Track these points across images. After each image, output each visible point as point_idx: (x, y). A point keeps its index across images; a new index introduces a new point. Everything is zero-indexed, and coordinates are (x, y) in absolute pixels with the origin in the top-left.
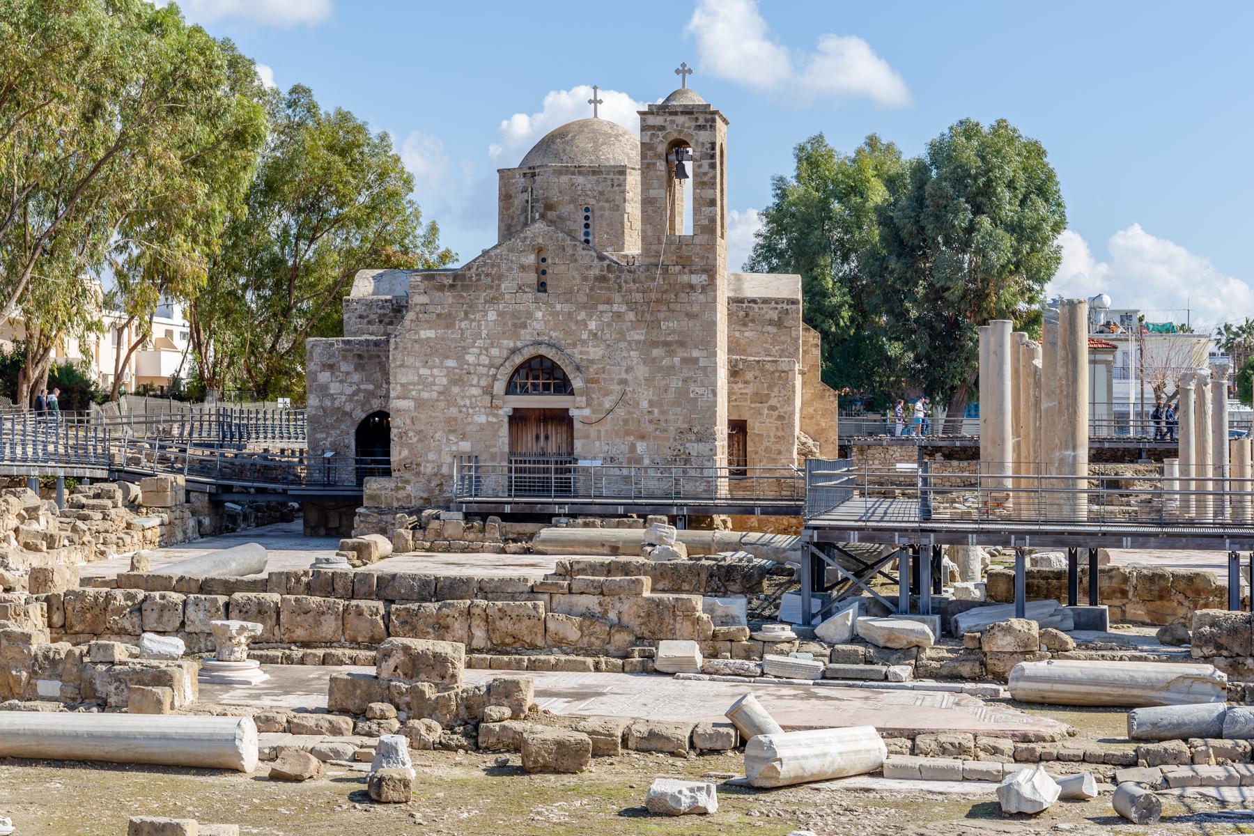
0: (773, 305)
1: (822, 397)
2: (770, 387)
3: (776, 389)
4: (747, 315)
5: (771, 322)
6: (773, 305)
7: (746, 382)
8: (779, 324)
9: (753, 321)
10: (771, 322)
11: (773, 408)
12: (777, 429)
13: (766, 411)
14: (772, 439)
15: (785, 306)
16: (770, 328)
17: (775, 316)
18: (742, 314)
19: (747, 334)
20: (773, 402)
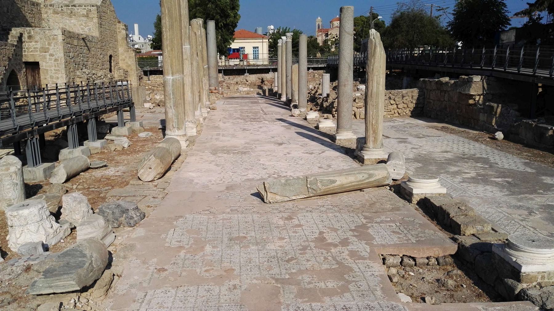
0: (83, 7)
1: (128, 51)
2: (49, 44)
3: (53, 45)
4: (71, 12)
5: (84, 16)
6: (83, 7)
7: (36, 42)
8: (87, 16)
9: (75, 15)
10: (84, 16)
11: (51, 55)
12: (55, 66)
13: (48, 57)
14: (53, 72)
15: (89, 8)
16: (83, 18)
17: (85, 12)
18: (69, 11)
19: (72, 21)
20: (51, 51)
